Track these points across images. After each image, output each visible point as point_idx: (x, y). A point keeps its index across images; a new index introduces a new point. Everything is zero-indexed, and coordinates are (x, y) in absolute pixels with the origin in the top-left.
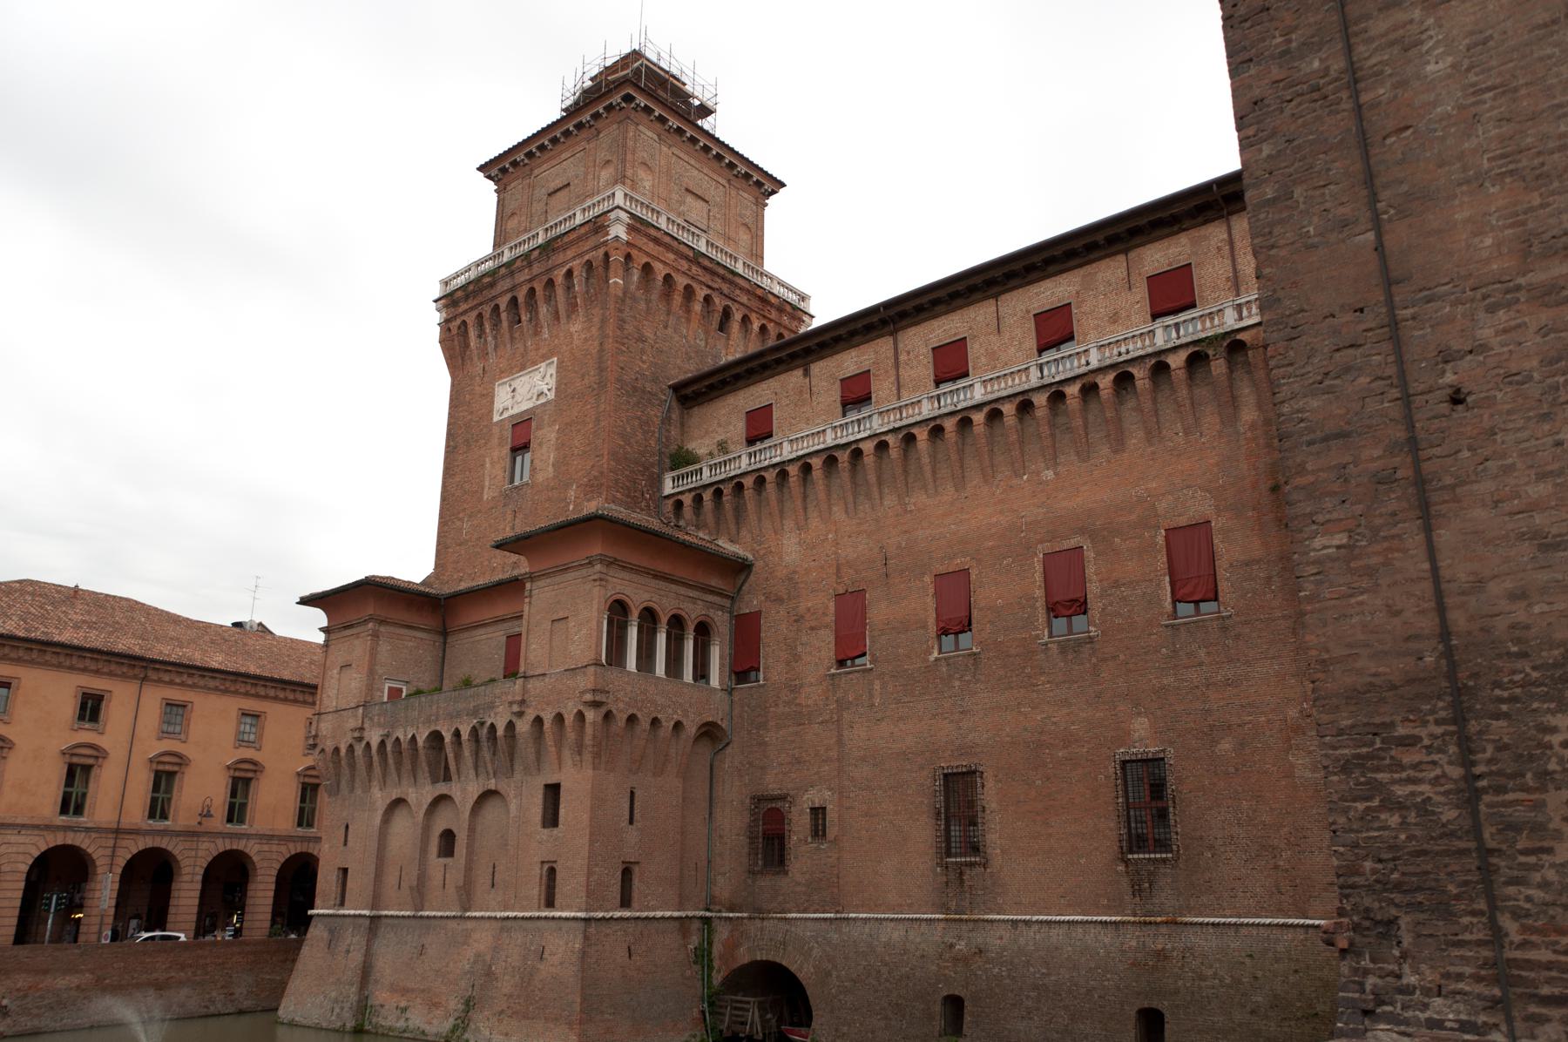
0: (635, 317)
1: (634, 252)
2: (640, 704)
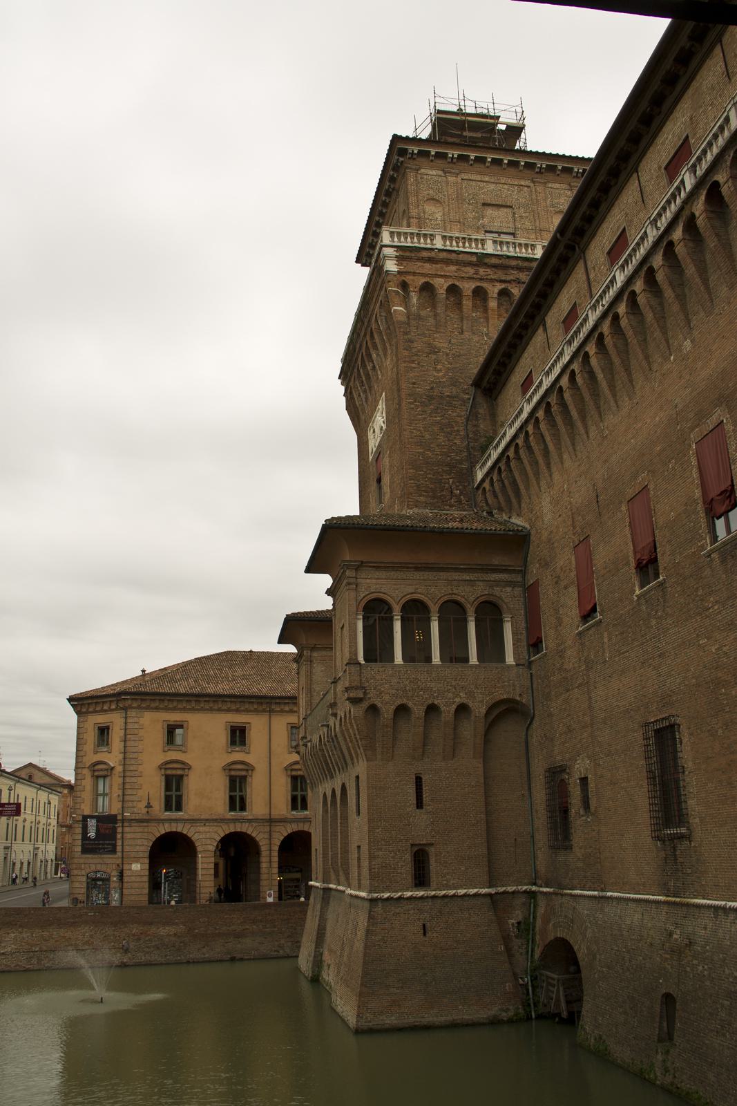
0: (424, 334)
1: (409, 279)
2: (410, 694)
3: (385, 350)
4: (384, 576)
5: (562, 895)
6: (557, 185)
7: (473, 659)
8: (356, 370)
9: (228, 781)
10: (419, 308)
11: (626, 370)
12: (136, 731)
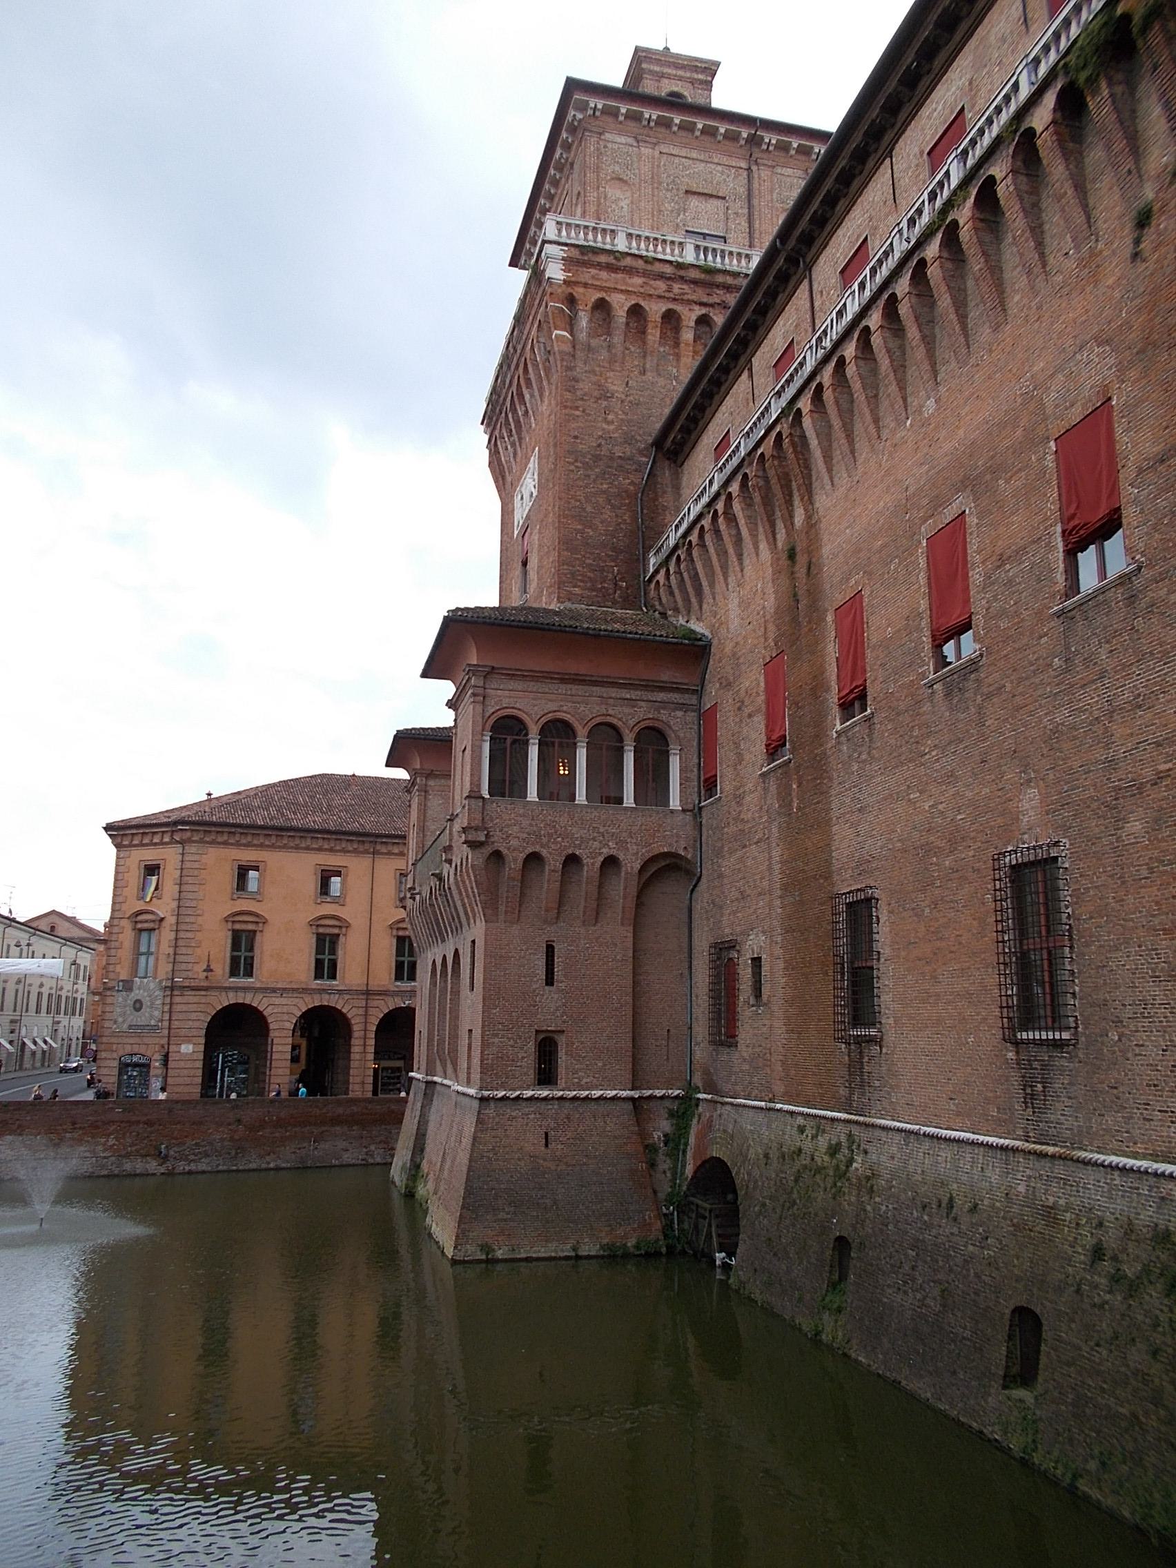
1: (578, 291)
2: (545, 840)
3: (541, 390)
4: (520, 688)
5: (723, 1104)
6: (790, 171)
7: (629, 800)
8: (503, 415)
9: (314, 940)
10: (589, 335)
11: (848, 436)
12: (196, 873)
